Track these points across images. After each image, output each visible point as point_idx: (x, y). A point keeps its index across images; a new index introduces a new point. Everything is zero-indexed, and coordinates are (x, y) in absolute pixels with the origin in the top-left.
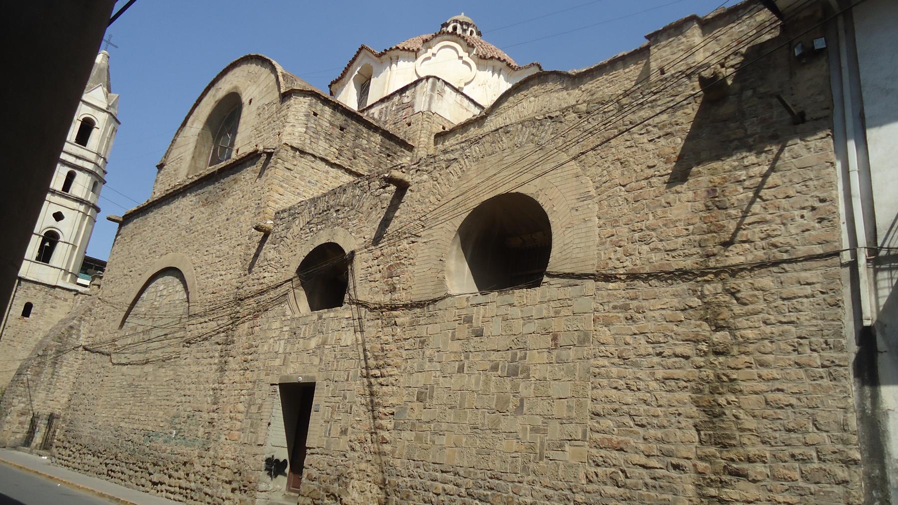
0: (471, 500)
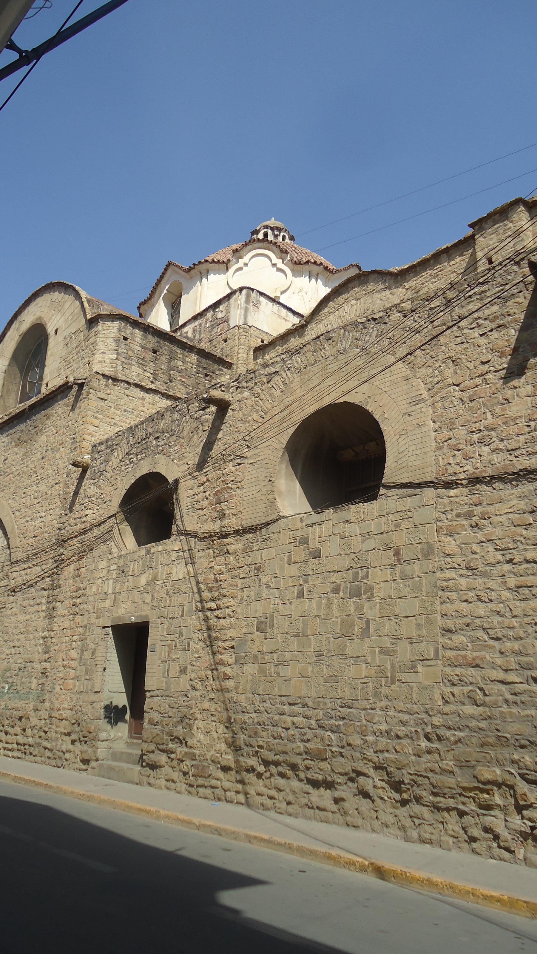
0: (322, 732)
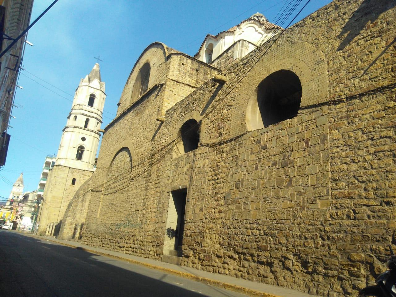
0: (266, 237)
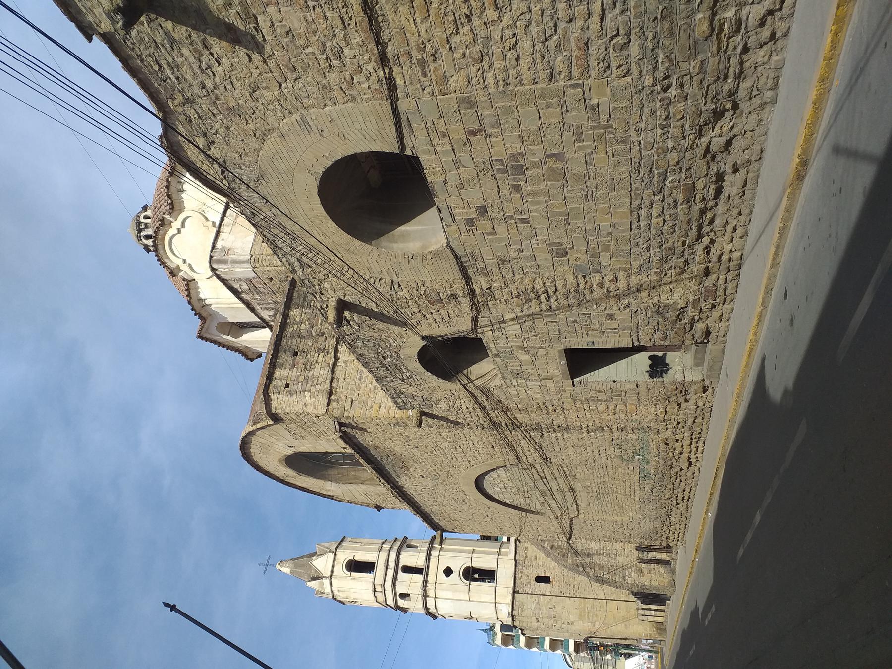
0: (666, 189)
